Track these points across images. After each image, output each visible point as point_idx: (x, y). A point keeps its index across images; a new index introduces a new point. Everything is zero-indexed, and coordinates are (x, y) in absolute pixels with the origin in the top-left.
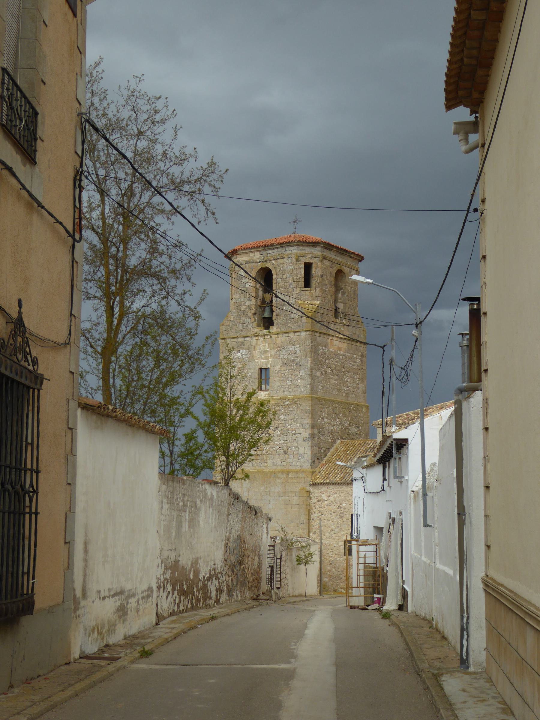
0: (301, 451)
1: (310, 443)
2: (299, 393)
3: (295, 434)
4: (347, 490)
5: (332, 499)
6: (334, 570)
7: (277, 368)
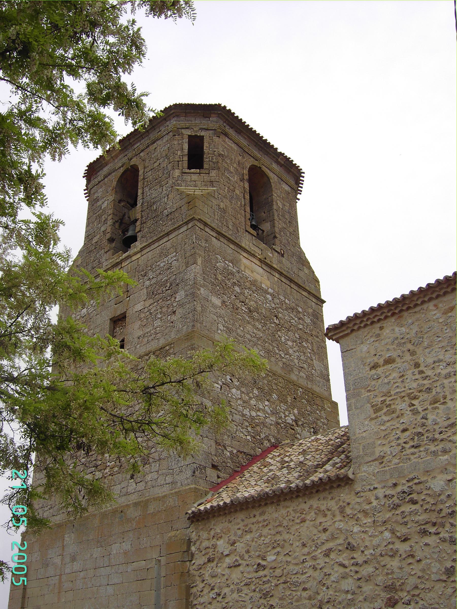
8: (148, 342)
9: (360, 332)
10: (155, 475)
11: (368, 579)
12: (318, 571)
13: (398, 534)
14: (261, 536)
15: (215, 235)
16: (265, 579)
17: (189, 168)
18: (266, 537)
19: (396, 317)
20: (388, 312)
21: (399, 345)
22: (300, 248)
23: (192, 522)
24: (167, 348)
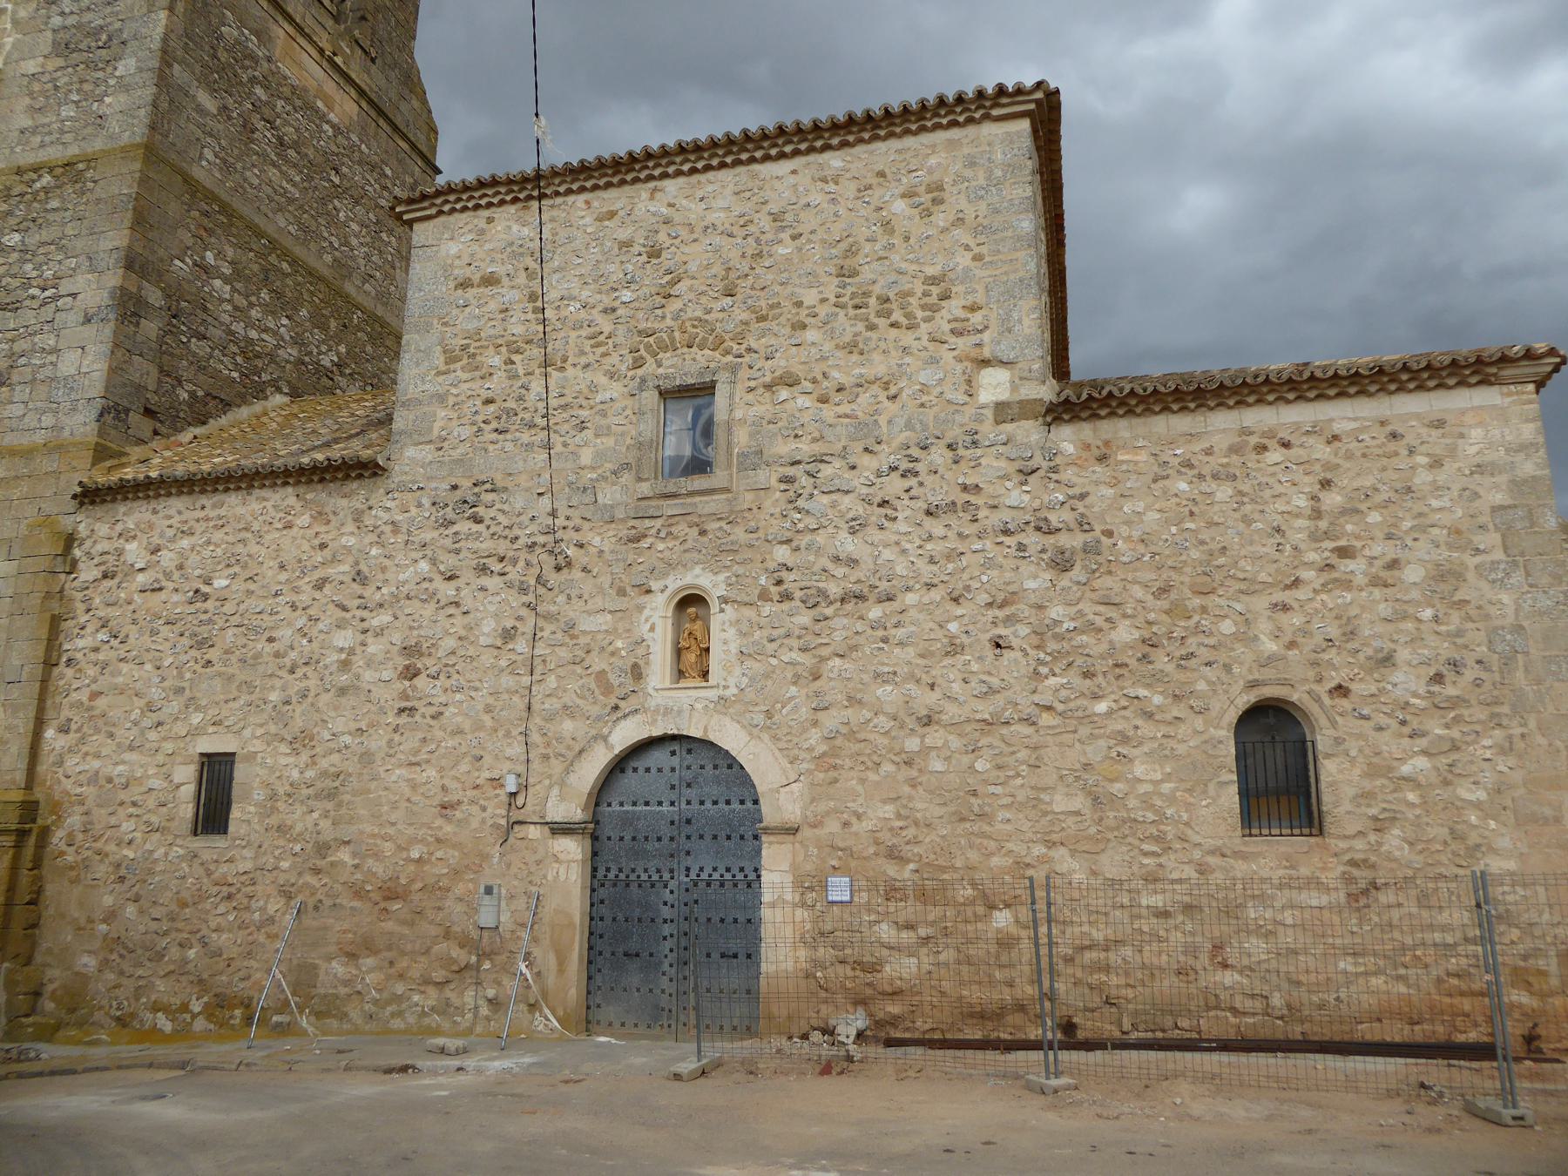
0: (68, 364)
1: (108, 330)
2: (98, 145)
3: (56, 298)
4: (240, 510)
5: (167, 558)
6: (131, 910)
7: (31, 66)
8: (42, 145)
9: (452, 218)
10: (17, 410)
11: (379, 633)
12: (299, 612)
13: (442, 568)
14: (209, 543)
16: (204, 617)
18: (217, 546)
19: (520, 205)
20: (507, 193)
21: (514, 255)
22: (412, 58)
23: (82, 504)
24: (81, 166)
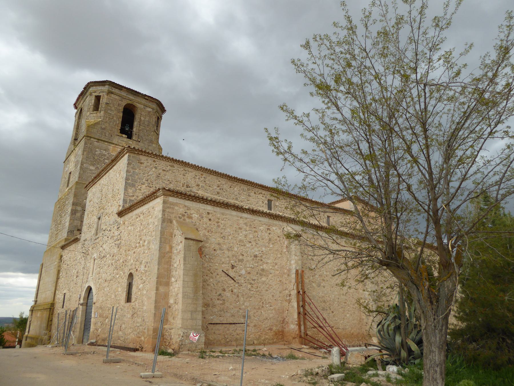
15: (96, 140)
17: (93, 111)
